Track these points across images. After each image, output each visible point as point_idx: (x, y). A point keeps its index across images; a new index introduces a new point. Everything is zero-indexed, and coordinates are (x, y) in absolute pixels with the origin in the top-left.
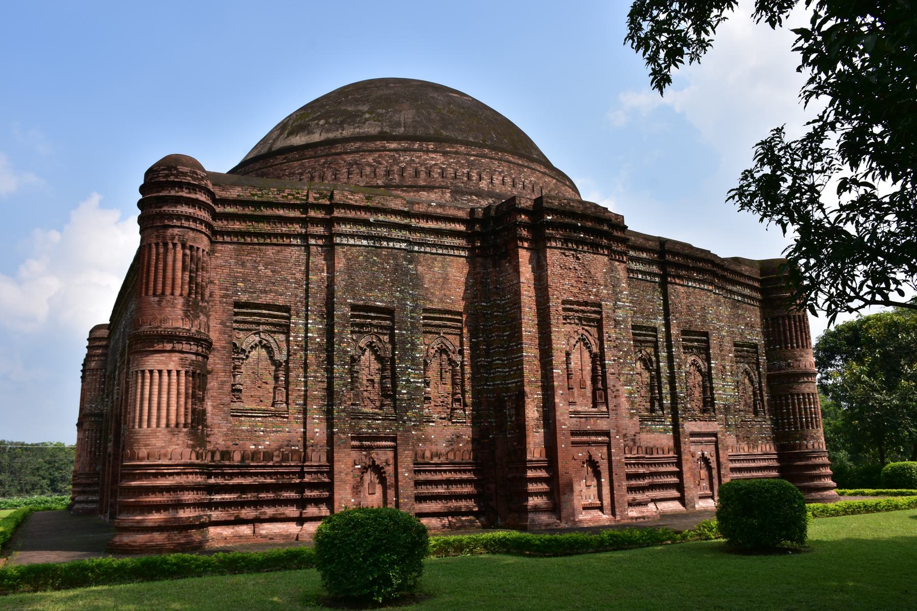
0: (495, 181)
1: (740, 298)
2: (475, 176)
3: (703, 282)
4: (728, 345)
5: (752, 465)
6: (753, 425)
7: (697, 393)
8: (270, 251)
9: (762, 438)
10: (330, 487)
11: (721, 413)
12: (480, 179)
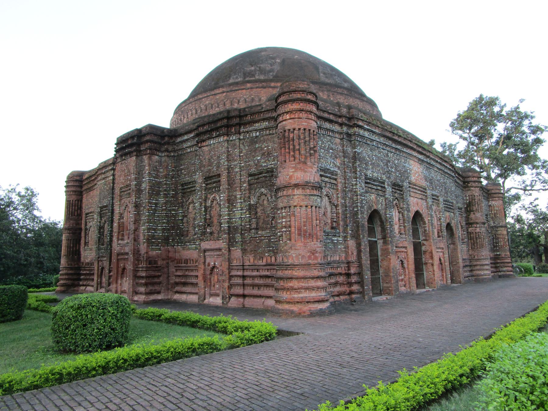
0: (189, 116)
2: (182, 118)
5: (255, 273)
8: (91, 193)
9: (270, 251)
10: (93, 274)
11: (226, 233)
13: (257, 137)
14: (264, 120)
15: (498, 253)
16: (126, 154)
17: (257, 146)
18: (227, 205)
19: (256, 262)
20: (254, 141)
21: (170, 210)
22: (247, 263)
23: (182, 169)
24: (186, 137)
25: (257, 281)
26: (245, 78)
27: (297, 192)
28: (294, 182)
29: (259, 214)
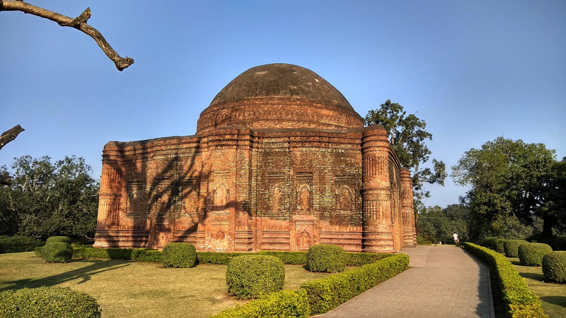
1: (343, 151)
3: (312, 147)
4: (329, 177)
5: (341, 237)
6: (346, 217)
7: (305, 202)
11: (317, 211)
12: (240, 115)
13: (342, 153)
14: (349, 143)
16: (222, 145)
17: (342, 158)
18: (318, 193)
19: (341, 230)
20: (338, 155)
21: (259, 191)
22: (334, 230)
23: (270, 163)
24: (273, 140)
25: (341, 241)
26: (292, 95)
27: (383, 192)
28: (381, 186)
29: (341, 200)
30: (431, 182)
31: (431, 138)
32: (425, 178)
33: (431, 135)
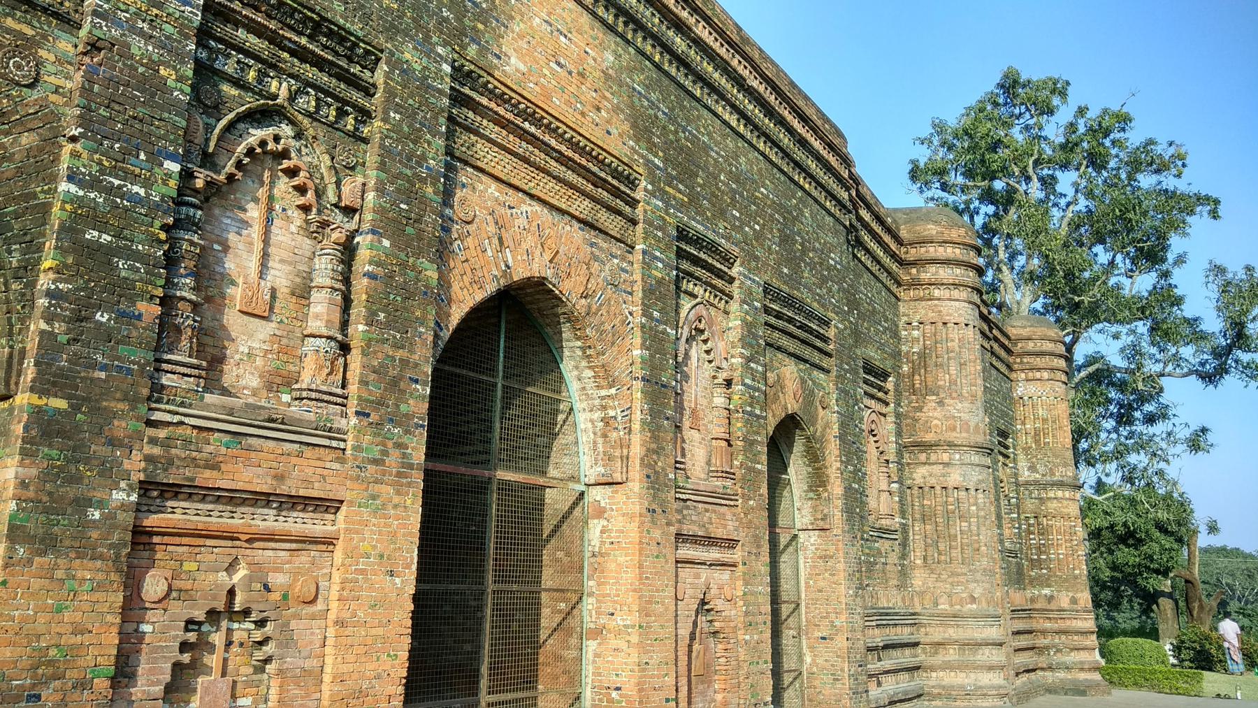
15: (1046, 591)
30: (1210, 377)
31: (1214, 215)
32: (1177, 359)
33: (1213, 205)
